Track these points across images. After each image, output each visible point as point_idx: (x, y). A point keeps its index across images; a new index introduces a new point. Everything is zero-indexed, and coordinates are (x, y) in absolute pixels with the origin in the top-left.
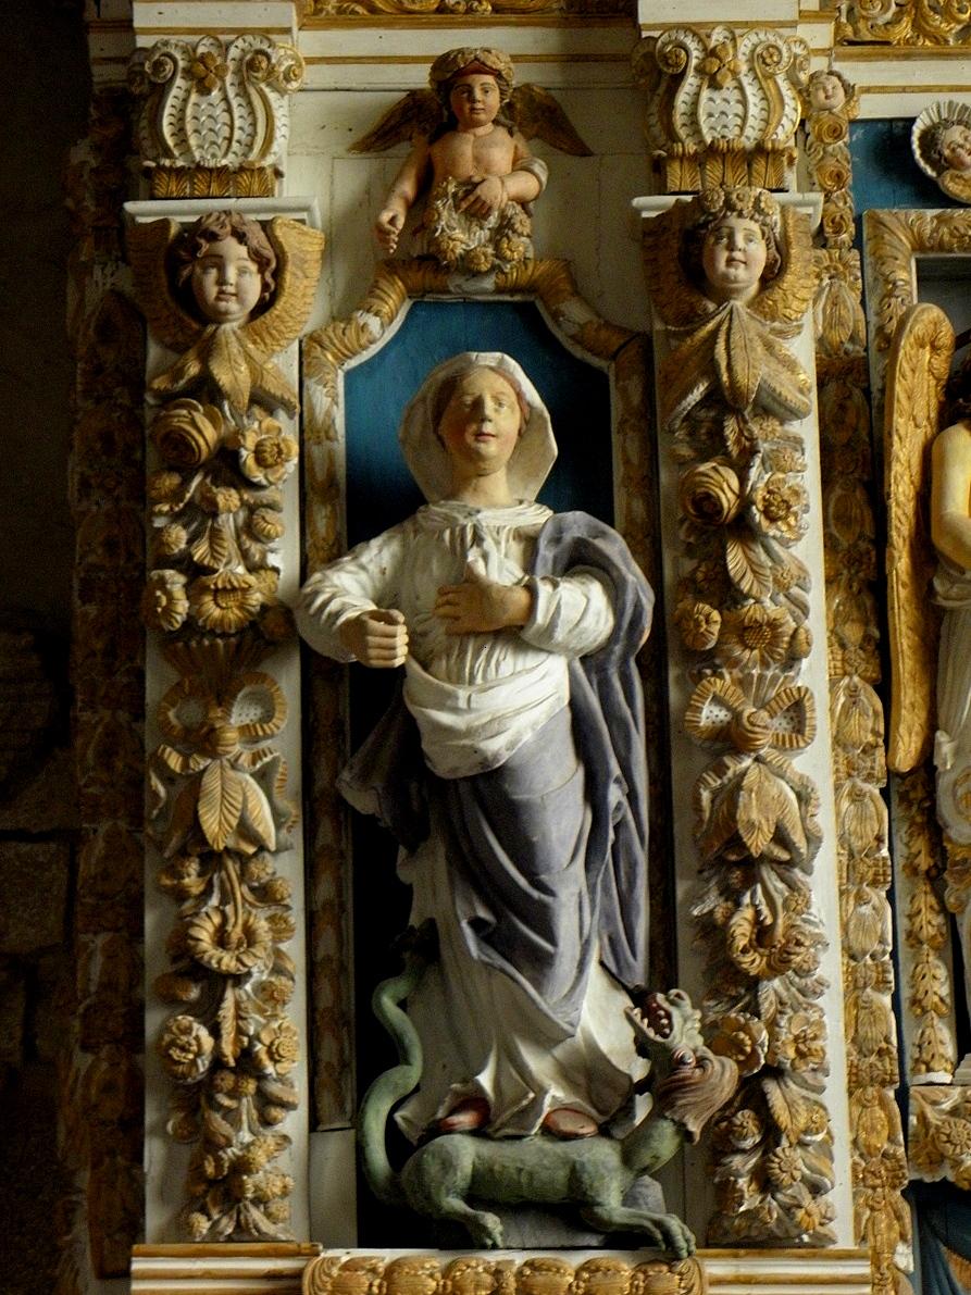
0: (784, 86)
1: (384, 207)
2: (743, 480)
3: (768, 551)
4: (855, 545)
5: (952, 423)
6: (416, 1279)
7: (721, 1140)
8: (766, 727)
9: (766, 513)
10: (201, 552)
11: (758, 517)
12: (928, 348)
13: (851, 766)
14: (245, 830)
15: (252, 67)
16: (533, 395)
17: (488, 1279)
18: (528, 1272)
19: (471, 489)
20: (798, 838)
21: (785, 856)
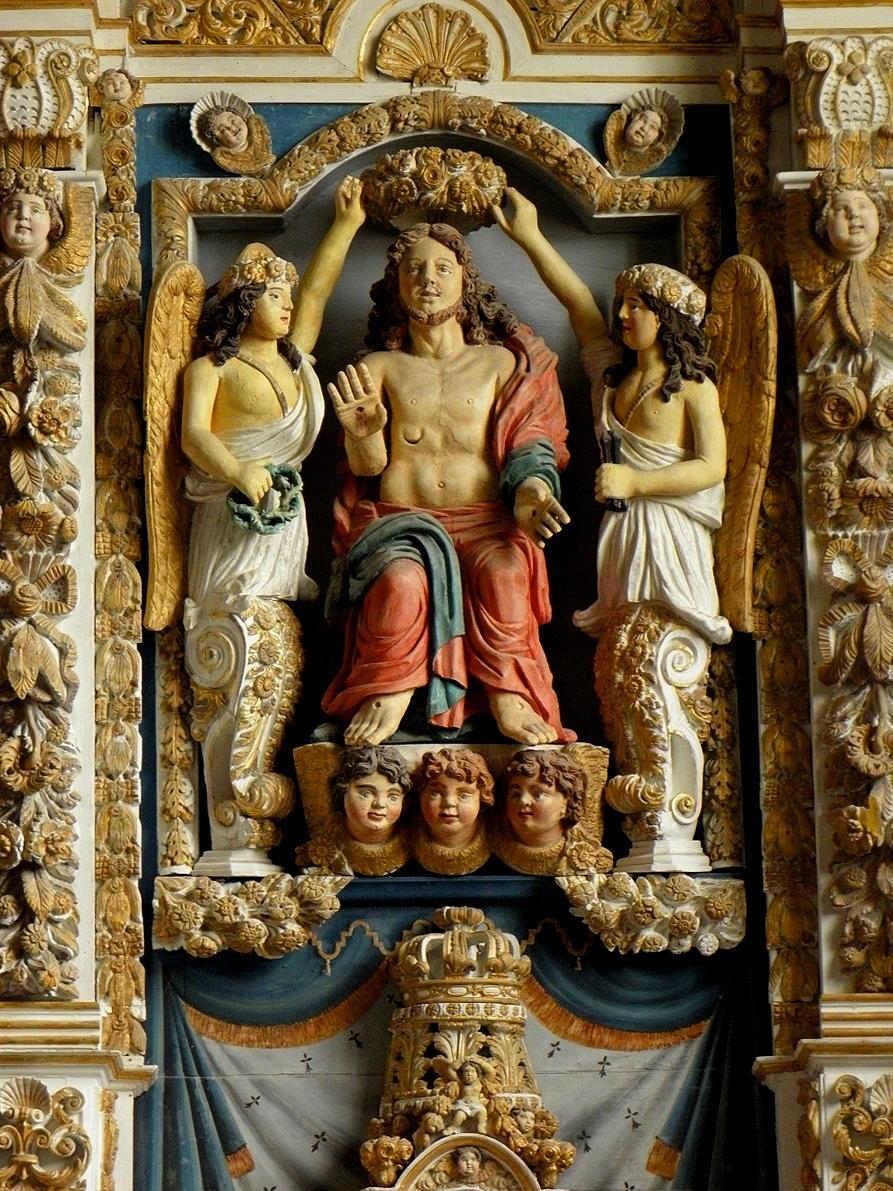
3: (46, 457)
4: (125, 450)
5: (203, 355)
8: (33, 598)
12: (182, 295)
21: (47, 698)
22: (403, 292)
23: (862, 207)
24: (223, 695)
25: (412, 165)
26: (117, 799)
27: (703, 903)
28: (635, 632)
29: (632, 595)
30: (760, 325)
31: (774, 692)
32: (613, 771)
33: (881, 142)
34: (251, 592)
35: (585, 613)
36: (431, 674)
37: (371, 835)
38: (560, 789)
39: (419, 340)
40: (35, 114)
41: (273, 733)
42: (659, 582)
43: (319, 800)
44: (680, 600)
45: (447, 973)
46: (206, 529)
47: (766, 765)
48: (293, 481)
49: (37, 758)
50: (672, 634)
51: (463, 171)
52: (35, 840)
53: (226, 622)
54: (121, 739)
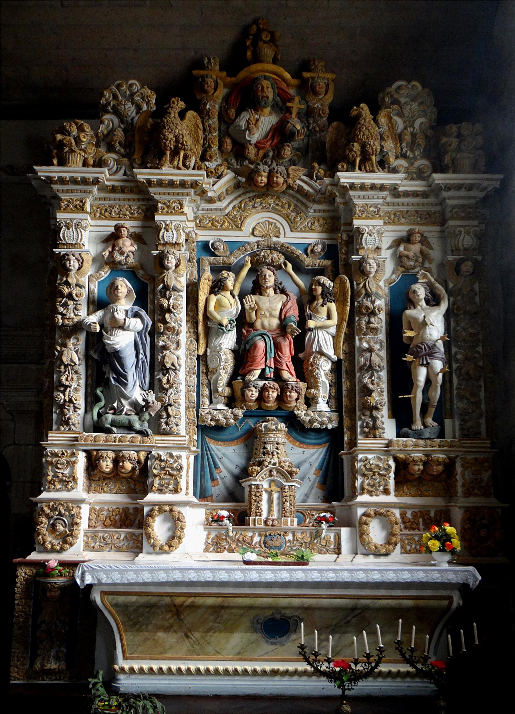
0: (182, 232)
2: (168, 302)
3: (174, 315)
5: (212, 294)
7: (159, 416)
9: (173, 308)
10: (65, 312)
11: (171, 308)
13: (190, 353)
14: (72, 361)
15: (77, 225)
16: (129, 285)
17: (113, 439)
22: (260, 281)
23: (373, 263)
24: (215, 370)
25: (263, 254)
27: (329, 418)
28: (314, 358)
29: (314, 350)
30: (346, 290)
31: (347, 372)
32: (307, 389)
33: (377, 250)
34: (223, 347)
35: (302, 354)
36: (266, 365)
37: (251, 401)
38: (296, 391)
39: (263, 293)
41: (228, 378)
42: (320, 347)
43: (238, 393)
44: (325, 351)
45: (268, 431)
46: (213, 333)
47: (344, 388)
48: (234, 322)
49: (171, 381)
50: (323, 358)
51: (275, 255)
53: (217, 354)
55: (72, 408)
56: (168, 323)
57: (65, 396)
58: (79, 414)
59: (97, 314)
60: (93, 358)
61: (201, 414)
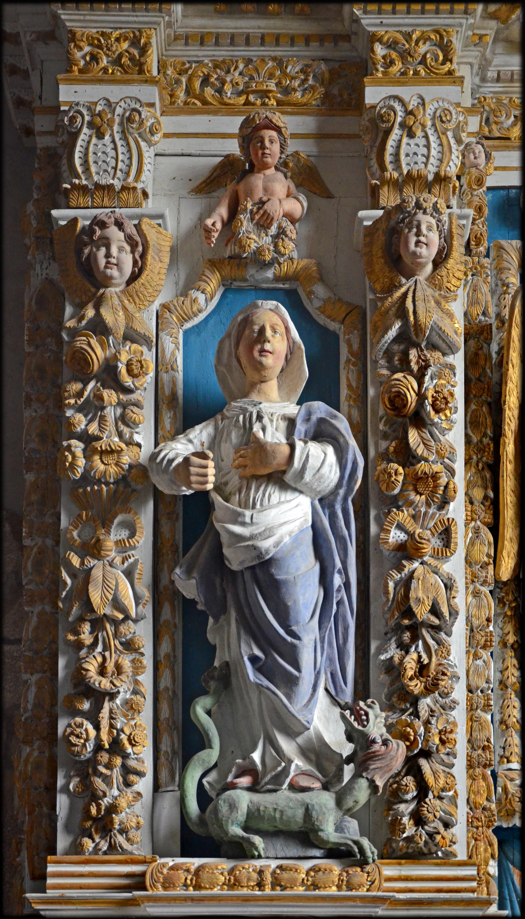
1: (209, 216)
6: (213, 876)
17: (255, 876)
18: (278, 871)
19: (256, 391)
20: (445, 610)
21: (437, 622)
26: (477, 709)
40: (424, 160)
52: (433, 731)
54: (479, 662)
55: (116, 774)
56: (419, 459)
57: (97, 727)
58: (139, 794)
59: (191, 436)
60: (176, 593)
61: (505, 789)
